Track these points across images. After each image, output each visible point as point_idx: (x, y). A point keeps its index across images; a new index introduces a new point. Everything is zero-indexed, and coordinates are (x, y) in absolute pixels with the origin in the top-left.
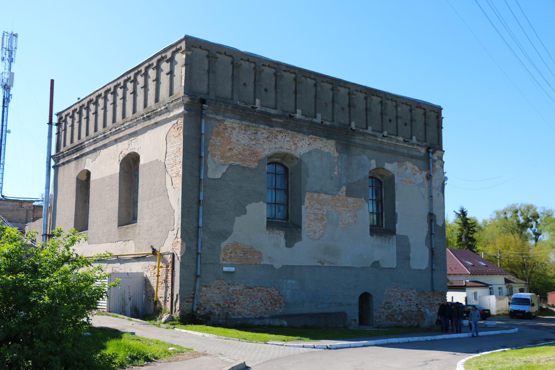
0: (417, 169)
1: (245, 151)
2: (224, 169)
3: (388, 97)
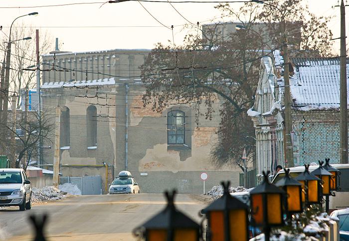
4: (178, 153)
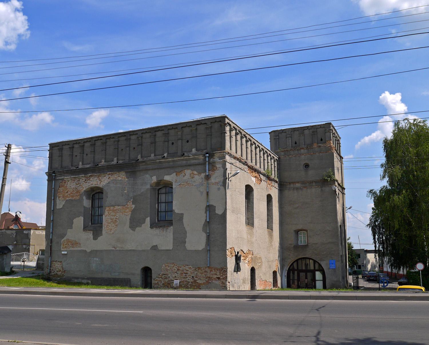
0: (195, 173)
1: (73, 191)
2: (63, 203)
3: (169, 127)
4: (92, 232)
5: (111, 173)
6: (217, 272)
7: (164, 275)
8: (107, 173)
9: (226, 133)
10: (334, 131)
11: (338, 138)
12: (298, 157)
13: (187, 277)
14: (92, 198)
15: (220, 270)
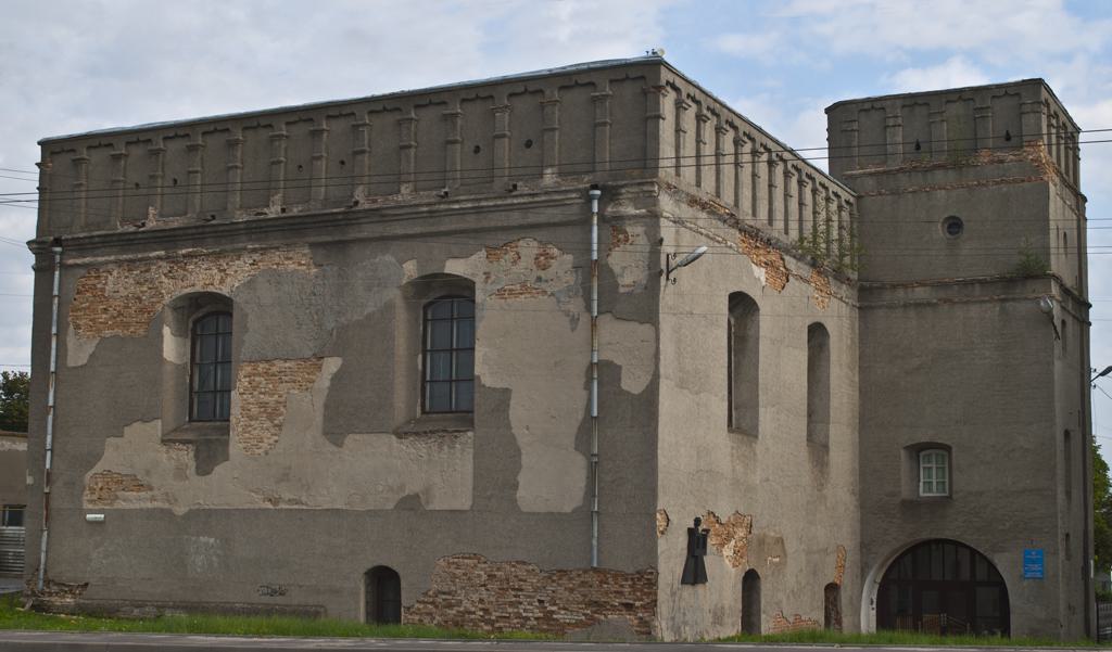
2: (90, 348)
5: (262, 249)
6: (622, 586)
7: (444, 593)
8: (245, 249)
9: (659, 117)
10: (1053, 107)
11: (1070, 129)
12: (924, 194)
13: (521, 603)
14: (194, 331)
15: (632, 579)
